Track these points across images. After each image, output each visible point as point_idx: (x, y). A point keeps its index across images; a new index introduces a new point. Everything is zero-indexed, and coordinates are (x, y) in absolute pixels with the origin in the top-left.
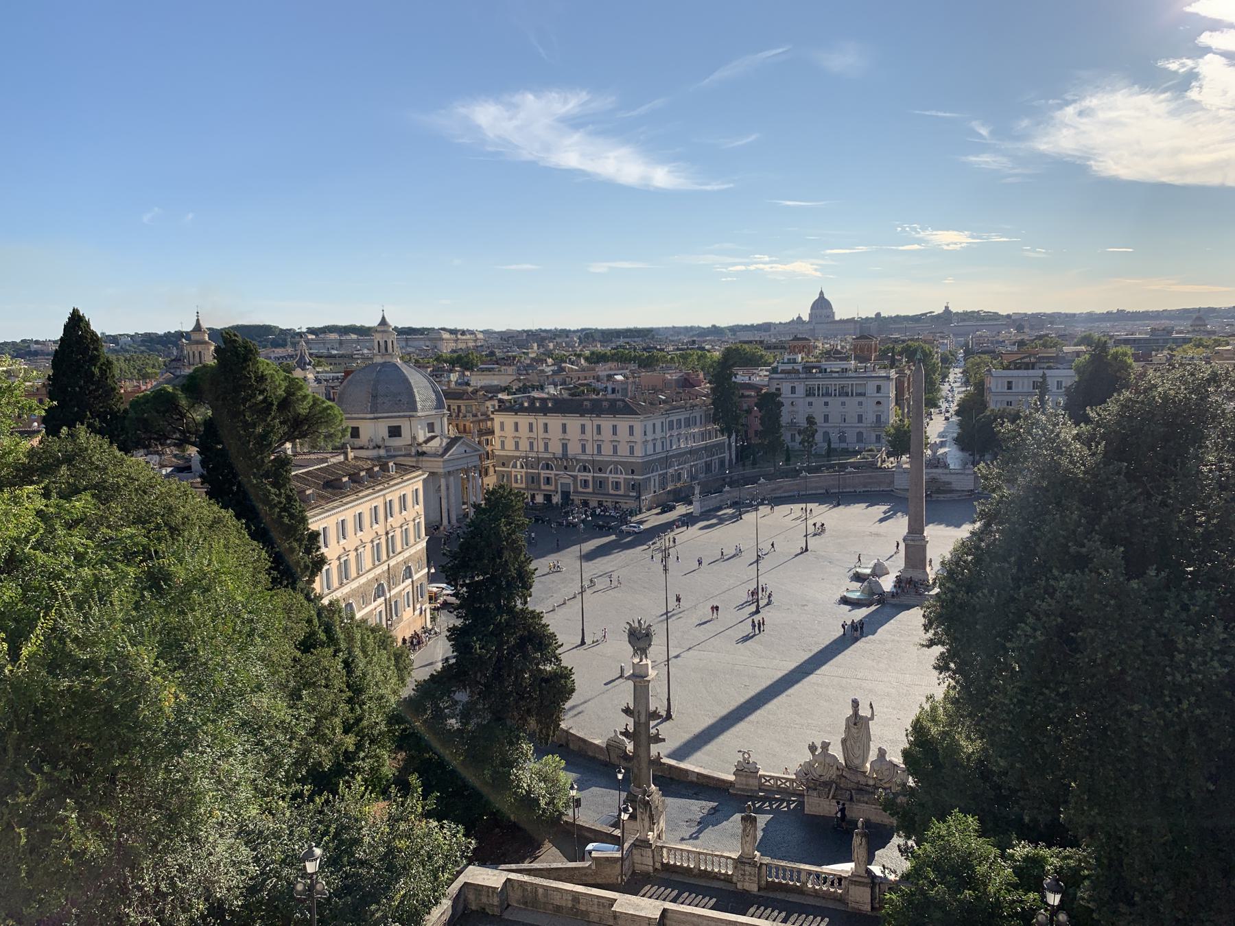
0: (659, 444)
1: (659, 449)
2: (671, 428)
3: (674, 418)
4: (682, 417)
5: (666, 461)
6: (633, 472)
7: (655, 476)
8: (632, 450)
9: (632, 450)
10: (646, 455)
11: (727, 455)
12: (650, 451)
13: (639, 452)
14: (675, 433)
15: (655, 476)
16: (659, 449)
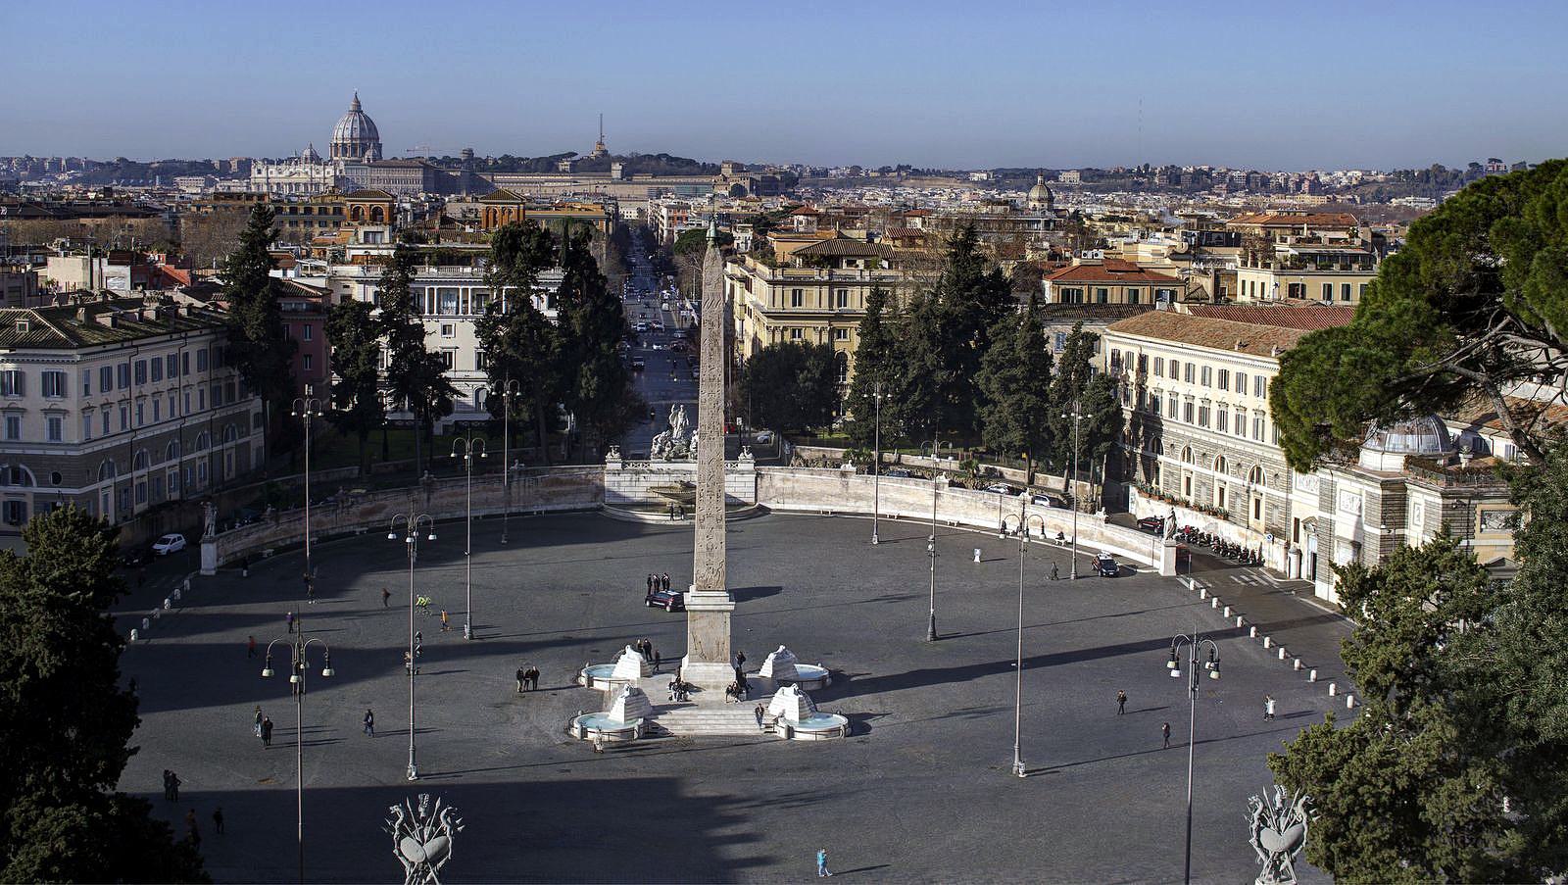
0: (115, 415)
1: (115, 427)
2: (141, 379)
3: (147, 357)
4: (163, 354)
5: (132, 454)
6: (57, 479)
7: (105, 488)
8: (55, 429)
9: (55, 429)
10: (89, 441)
11: (256, 438)
12: (97, 431)
13: (72, 432)
14: (149, 387)
15: (105, 488)
16: (115, 427)
